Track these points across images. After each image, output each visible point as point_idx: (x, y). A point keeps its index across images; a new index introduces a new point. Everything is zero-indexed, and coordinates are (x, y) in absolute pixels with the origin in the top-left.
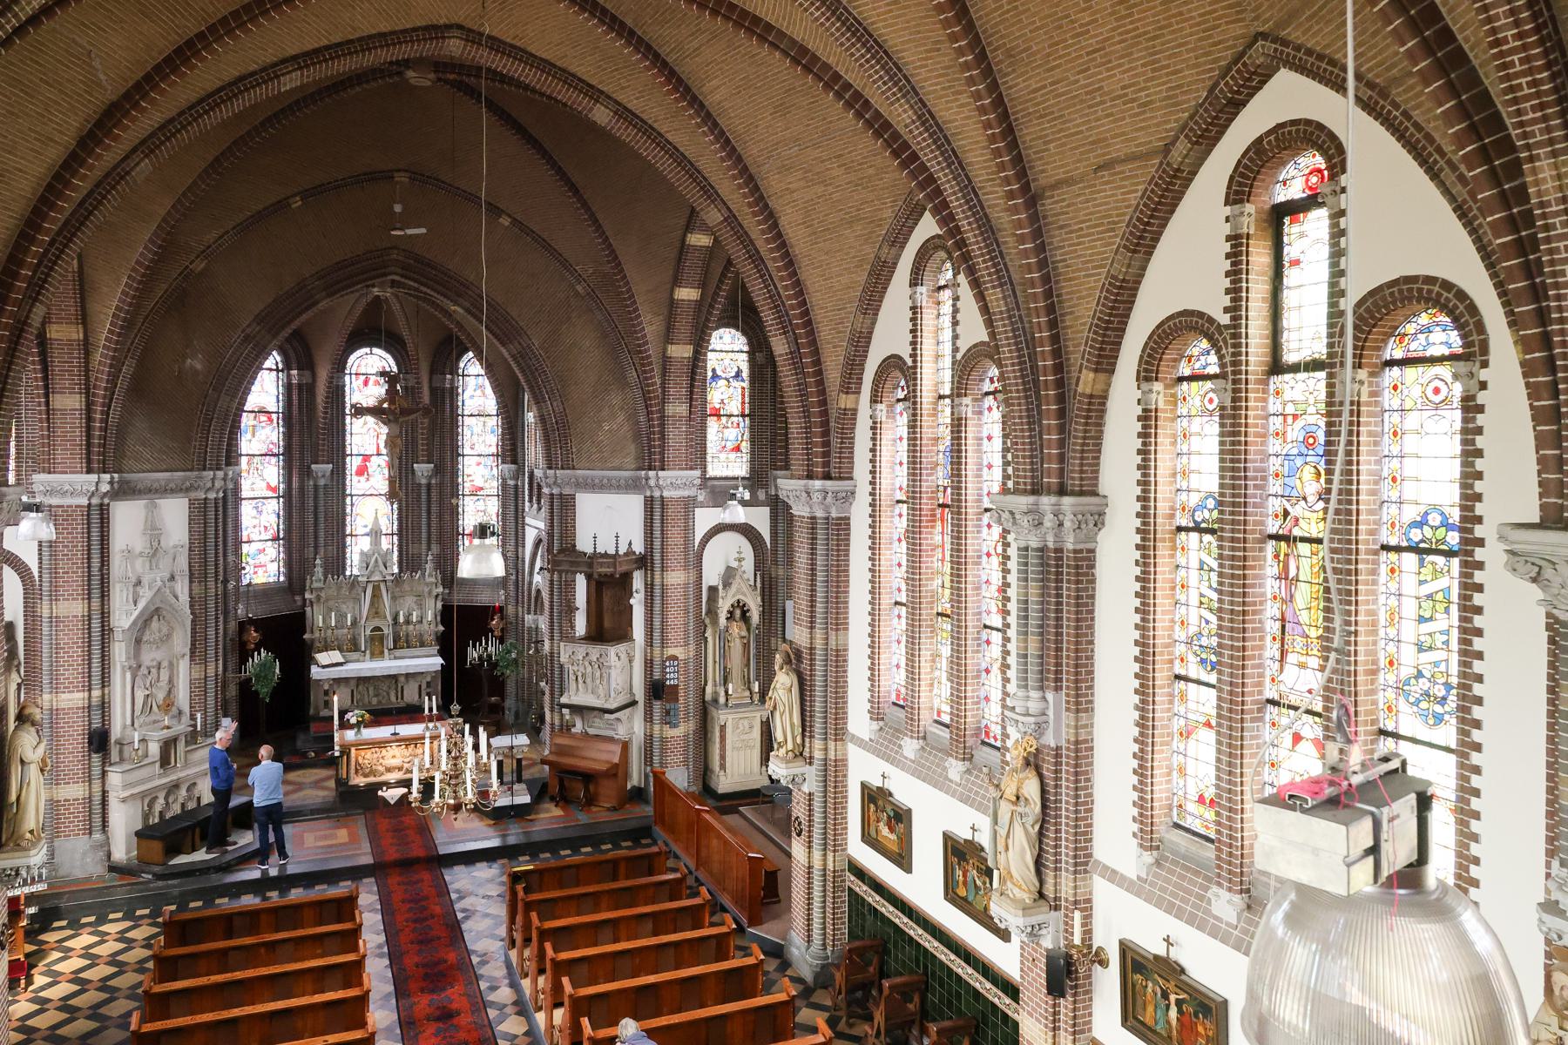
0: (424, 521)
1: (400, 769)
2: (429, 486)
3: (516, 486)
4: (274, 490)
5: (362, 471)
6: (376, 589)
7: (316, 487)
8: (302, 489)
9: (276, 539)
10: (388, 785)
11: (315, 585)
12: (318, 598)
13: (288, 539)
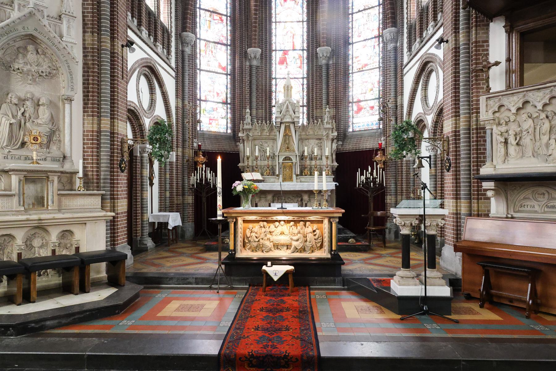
0: (324, 91)
1: (288, 247)
2: (327, 65)
4: (224, 69)
5: (283, 61)
6: (287, 128)
7: (251, 66)
8: (241, 67)
9: (225, 103)
10: (276, 261)
11: (246, 127)
12: (248, 136)
13: (233, 104)
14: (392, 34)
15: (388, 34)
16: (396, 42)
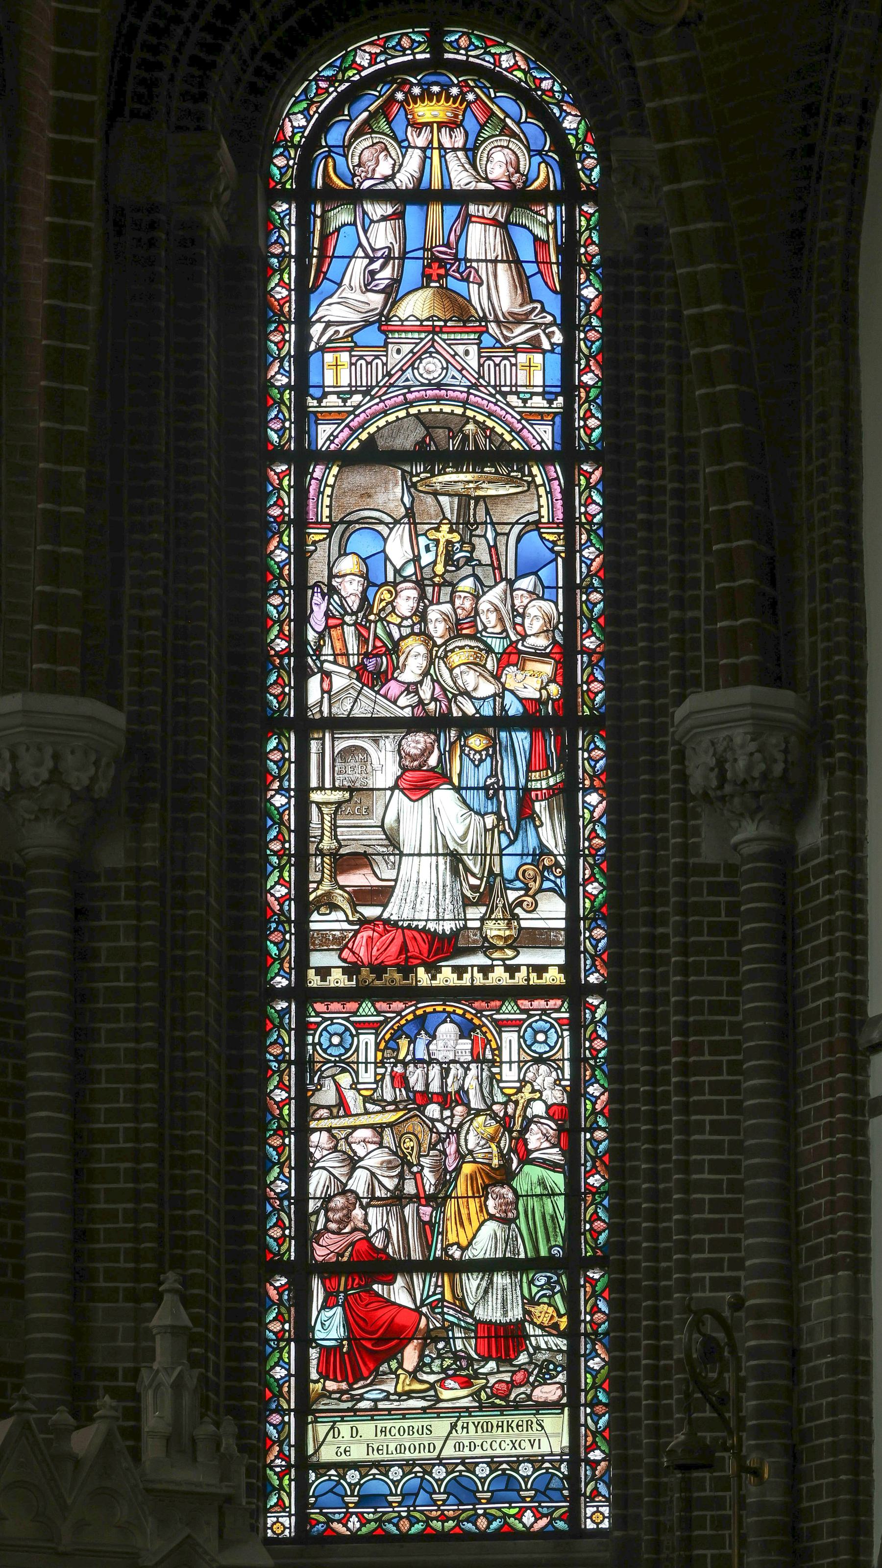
3: (782, 859)
14: (774, 740)
15: (739, 735)
16: (794, 815)
